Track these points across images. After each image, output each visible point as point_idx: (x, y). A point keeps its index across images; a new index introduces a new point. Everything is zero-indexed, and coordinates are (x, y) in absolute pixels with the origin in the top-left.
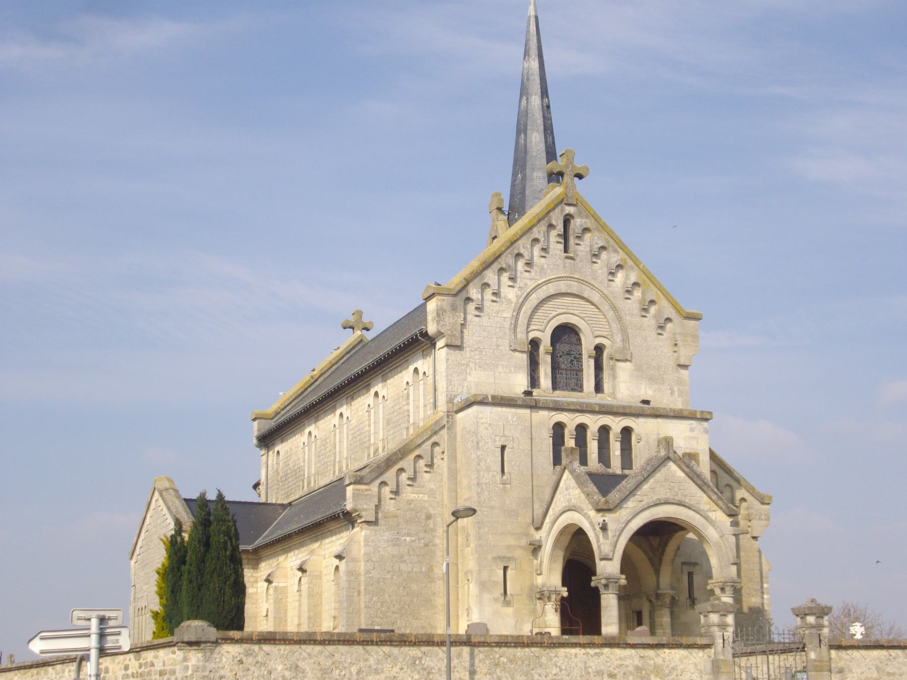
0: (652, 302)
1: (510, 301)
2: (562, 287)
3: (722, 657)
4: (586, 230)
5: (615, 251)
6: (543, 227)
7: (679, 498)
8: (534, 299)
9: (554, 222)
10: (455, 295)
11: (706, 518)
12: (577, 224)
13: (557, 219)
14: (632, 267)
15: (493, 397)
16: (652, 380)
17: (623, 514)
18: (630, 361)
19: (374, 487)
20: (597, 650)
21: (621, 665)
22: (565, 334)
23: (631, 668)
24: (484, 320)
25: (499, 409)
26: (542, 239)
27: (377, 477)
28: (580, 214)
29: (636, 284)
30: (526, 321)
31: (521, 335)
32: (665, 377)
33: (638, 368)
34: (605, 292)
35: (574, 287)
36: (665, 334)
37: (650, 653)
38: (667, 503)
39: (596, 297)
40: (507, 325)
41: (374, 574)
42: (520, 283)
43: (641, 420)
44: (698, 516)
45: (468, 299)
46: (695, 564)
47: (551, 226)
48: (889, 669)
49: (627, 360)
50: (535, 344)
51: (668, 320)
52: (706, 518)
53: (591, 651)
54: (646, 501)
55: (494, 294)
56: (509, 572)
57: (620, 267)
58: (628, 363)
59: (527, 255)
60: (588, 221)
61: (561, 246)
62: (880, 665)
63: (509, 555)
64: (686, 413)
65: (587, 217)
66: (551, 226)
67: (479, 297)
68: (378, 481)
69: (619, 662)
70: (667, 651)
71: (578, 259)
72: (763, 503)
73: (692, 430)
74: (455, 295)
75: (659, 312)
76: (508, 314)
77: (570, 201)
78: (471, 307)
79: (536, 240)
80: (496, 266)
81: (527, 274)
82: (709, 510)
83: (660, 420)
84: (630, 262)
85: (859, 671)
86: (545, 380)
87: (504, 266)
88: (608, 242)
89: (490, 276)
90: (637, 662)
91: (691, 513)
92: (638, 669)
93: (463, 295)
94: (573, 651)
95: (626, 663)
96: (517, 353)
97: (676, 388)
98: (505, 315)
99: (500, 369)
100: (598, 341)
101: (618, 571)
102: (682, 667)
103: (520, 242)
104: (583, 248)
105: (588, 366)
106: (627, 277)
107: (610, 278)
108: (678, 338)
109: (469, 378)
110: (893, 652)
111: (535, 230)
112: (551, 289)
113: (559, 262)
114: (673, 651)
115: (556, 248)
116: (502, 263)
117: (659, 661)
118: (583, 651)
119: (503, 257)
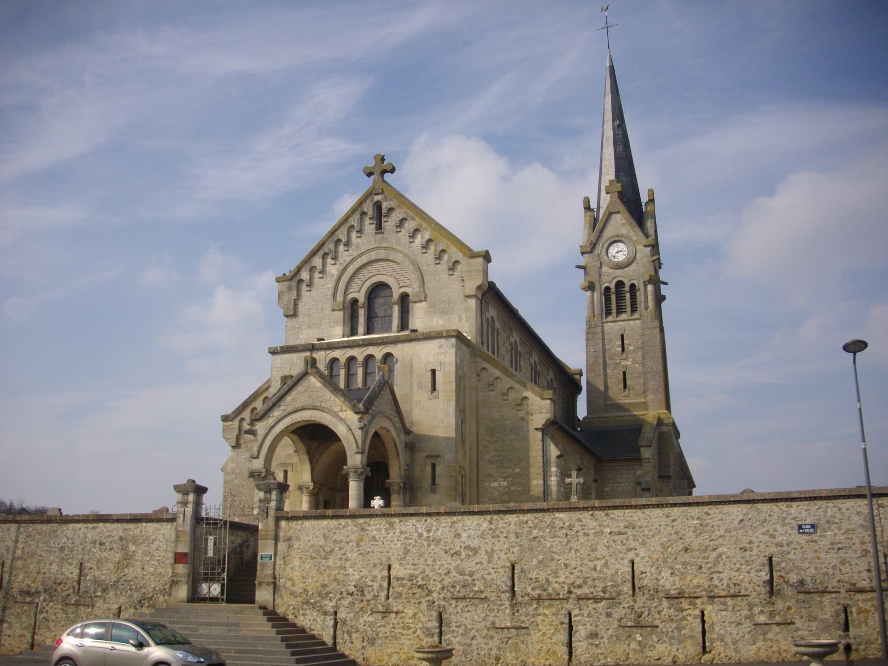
0: (443, 251)
1: (332, 275)
2: (373, 256)
3: (181, 529)
4: (391, 210)
5: (413, 219)
6: (357, 216)
7: (317, 403)
8: (351, 270)
9: (366, 210)
10: (291, 279)
11: (336, 416)
12: (385, 206)
13: (368, 208)
14: (426, 228)
15: (282, 347)
16: (443, 312)
17: (271, 421)
18: (425, 300)
19: (236, 423)
20: (95, 525)
21: (110, 536)
22: (378, 289)
23: (116, 538)
24: (314, 293)
25: (287, 356)
26: (356, 225)
27: (237, 415)
28: (385, 199)
29: (429, 241)
30: (344, 288)
31: (340, 298)
32: (455, 308)
33: (432, 305)
34: (406, 251)
35: (382, 254)
36: (456, 274)
37: (132, 526)
38: (303, 409)
39: (399, 257)
40: (330, 292)
41: (236, 482)
42: (341, 260)
43: (399, 346)
44: (329, 417)
45: (301, 281)
46: (439, 456)
47: (364, 214)
48: (336, 537)
49: (421, 301)
50: (355, 301)
51: (456, 262)
52: (336, 416)
53: (90, 526)
54: (290, 409)
55: (320, 272)
56: (289, 474)
57: (416, 230)
58: (424, 303)
59: (344, 239)
60: (391, 202)
61: (374, 226)
62: (328, 534)
63: (288, 461)
64: (433, 335)
65: (391, 200)
66: (364, 214)
67: (308, 277)
68: (239, 418)
69: (109, 534)
70: (144, 524)
71: (386, 233)
72: (543, 399)
73: (441, 347)
74: (291, 279)
75: (449, 257)
76: (331, 285)
77: (377, 191)
78: (304, 287)
79: (353, 226)
80: (321, 253)
81: (346, 253)
82: (341, 411)
83: (413, 343)
84: (424, 225)
85: (307, 539)
86: (361, 328)
87: (327, 251)
88: (407, 213)
89: (317, 261)
90: (121, 534)
91: (325, 415)
92: (121, 538)
93: (297, 279)
94: (79, 525)
95: (113, 534)
96: (336, 313)
97: (464, 316)
98: (329, 286)
99: (323, 326)
100: (402, 290)
101: (262, 466)
102: (154, 537)
103: (339, 231)
104: (389, 224)
105: (396, 309)
106: (422, 237)
107: (411, 240)
108: (464, 274)
109: (301, 337)
110: (342, 522)
111: (351, 219)
112: (364, 260)
113: (372, 238)
114: (148, 524)
115: (369, 227)
116: (325, 249)
117: (137, 532)
118: (85, 525)
119: (326, 245)
